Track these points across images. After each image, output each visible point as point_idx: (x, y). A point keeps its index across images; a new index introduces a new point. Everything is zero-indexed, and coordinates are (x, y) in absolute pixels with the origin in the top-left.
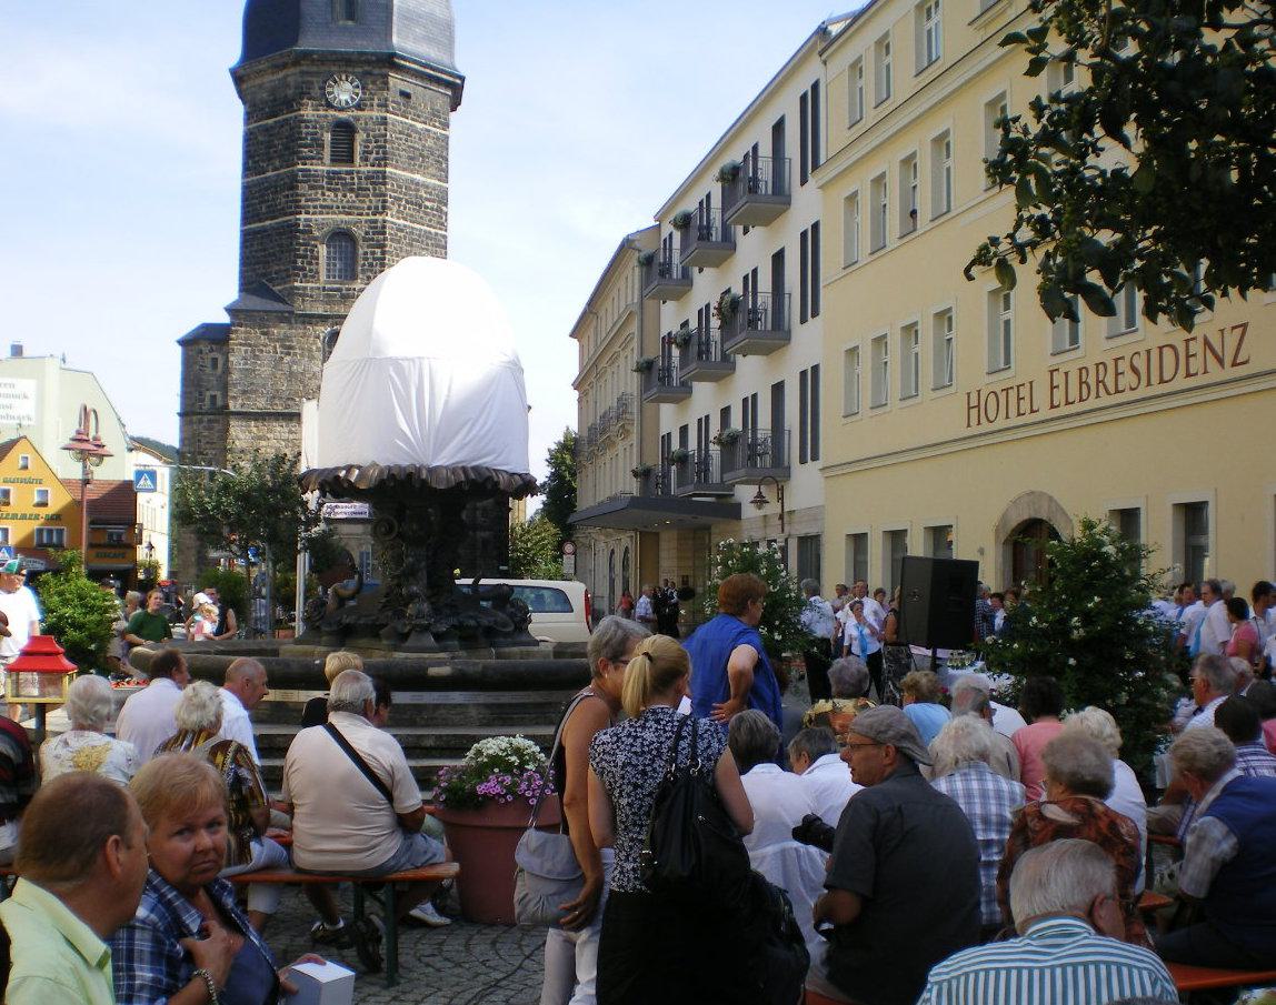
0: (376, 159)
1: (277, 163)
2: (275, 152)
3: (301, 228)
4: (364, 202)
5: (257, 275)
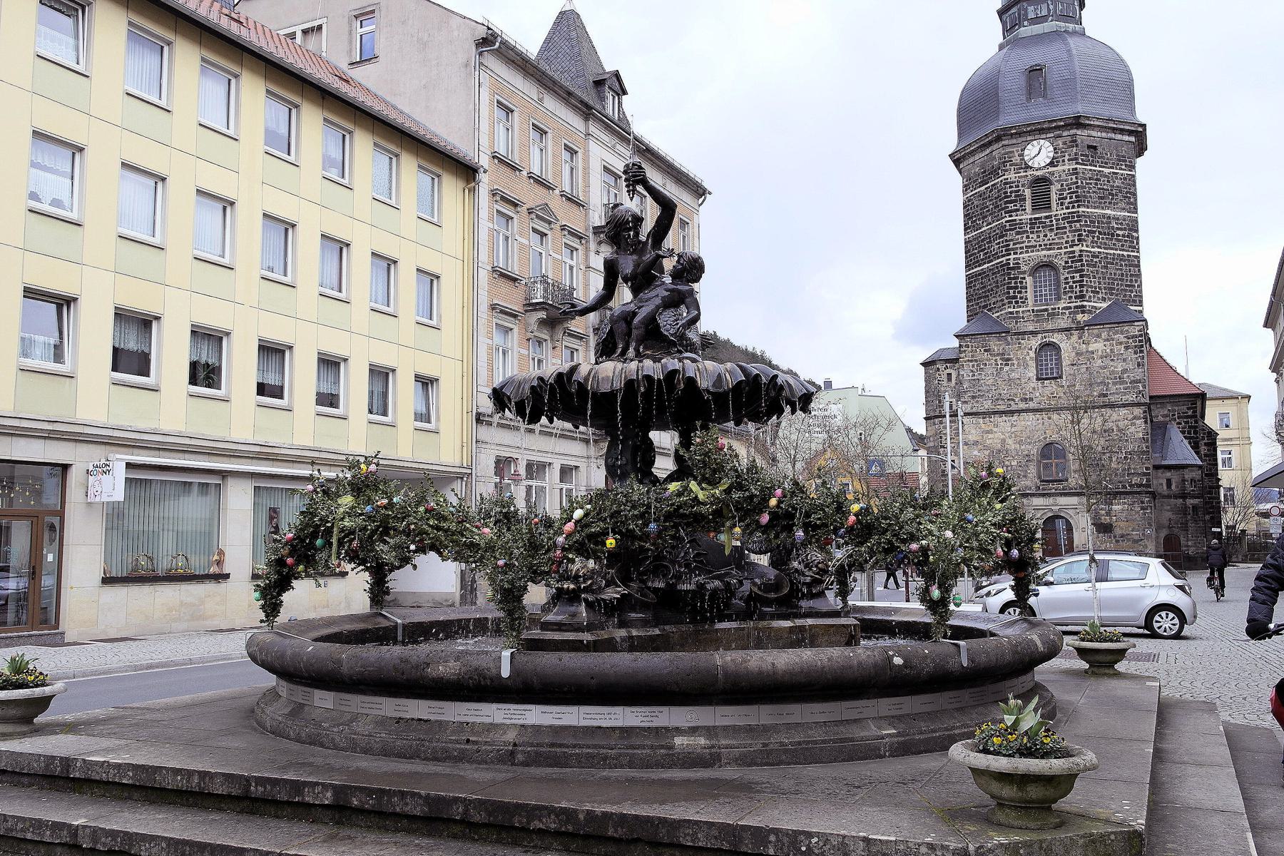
0: (1069, 203)
2: (988, 211)
5: (980, 307)
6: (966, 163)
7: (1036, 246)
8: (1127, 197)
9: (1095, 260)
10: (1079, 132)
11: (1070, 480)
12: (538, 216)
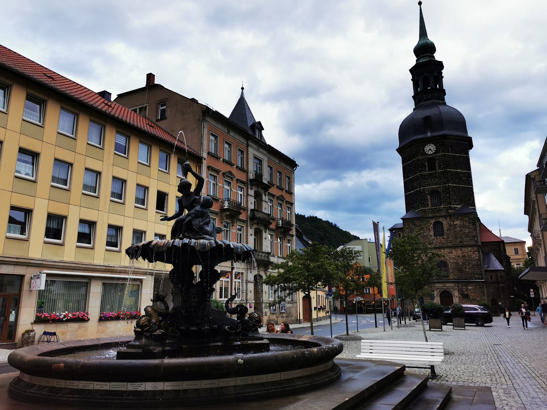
4: (441, 181)
7: (431, 184)
10: (445, 141)
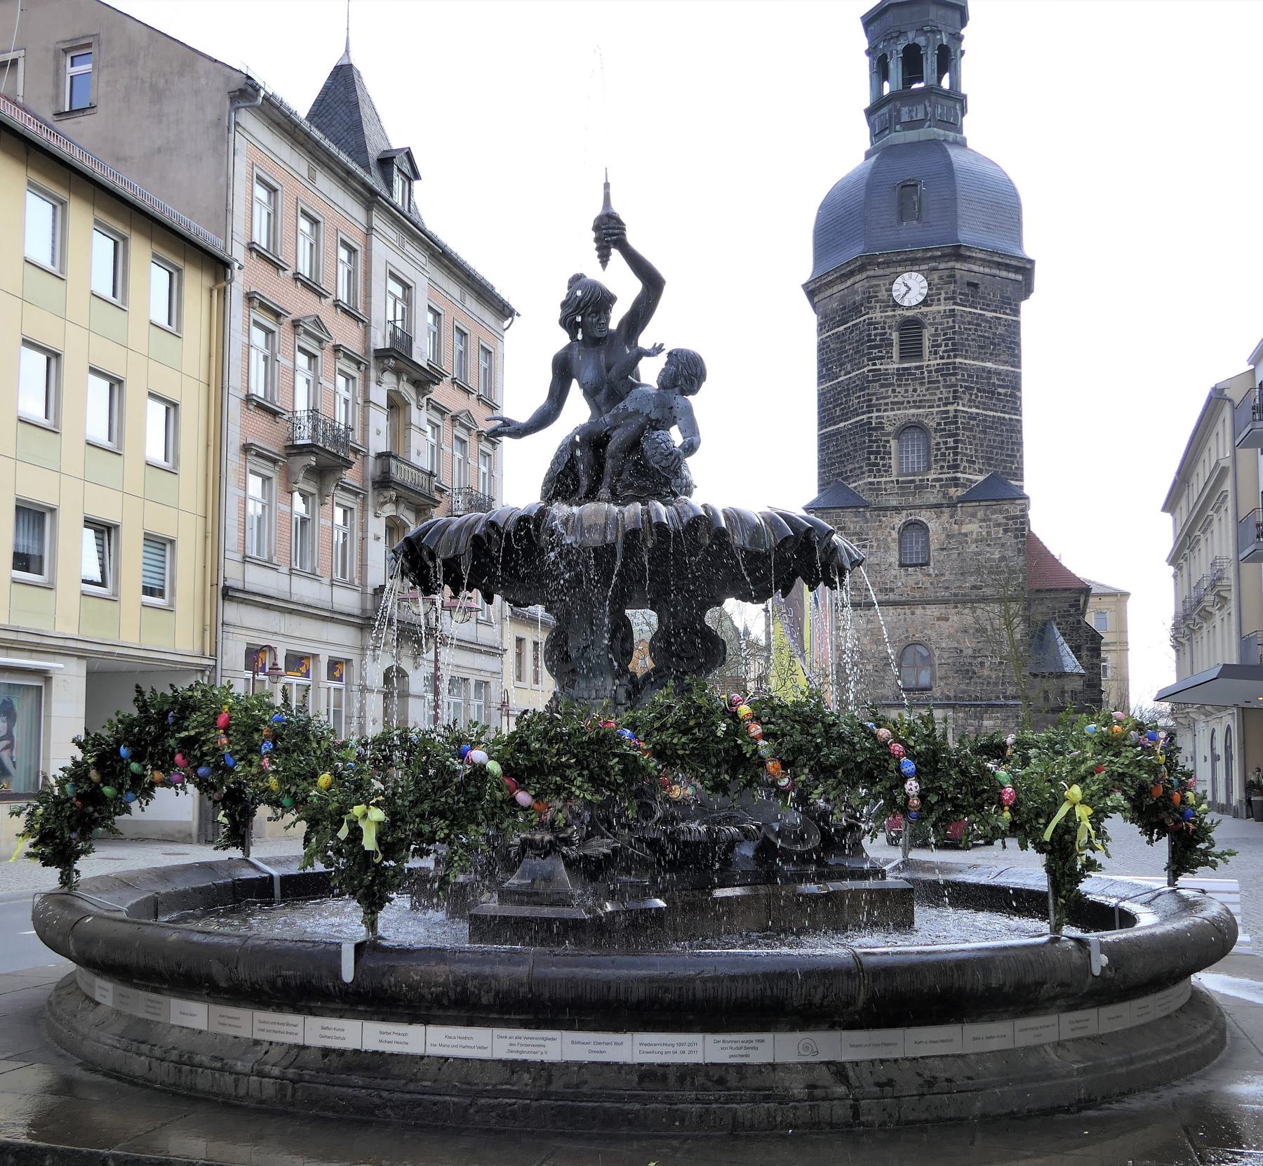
0: (944, 352)
1: (849, 367)
2: (847, 356)
3: (874, 425)
6: (822, 296)
7: (903, 403)
8: (1011, 348)
9: (972, 422)
10: (958, 265)
11: (934, 689)
12: (307, 332)
